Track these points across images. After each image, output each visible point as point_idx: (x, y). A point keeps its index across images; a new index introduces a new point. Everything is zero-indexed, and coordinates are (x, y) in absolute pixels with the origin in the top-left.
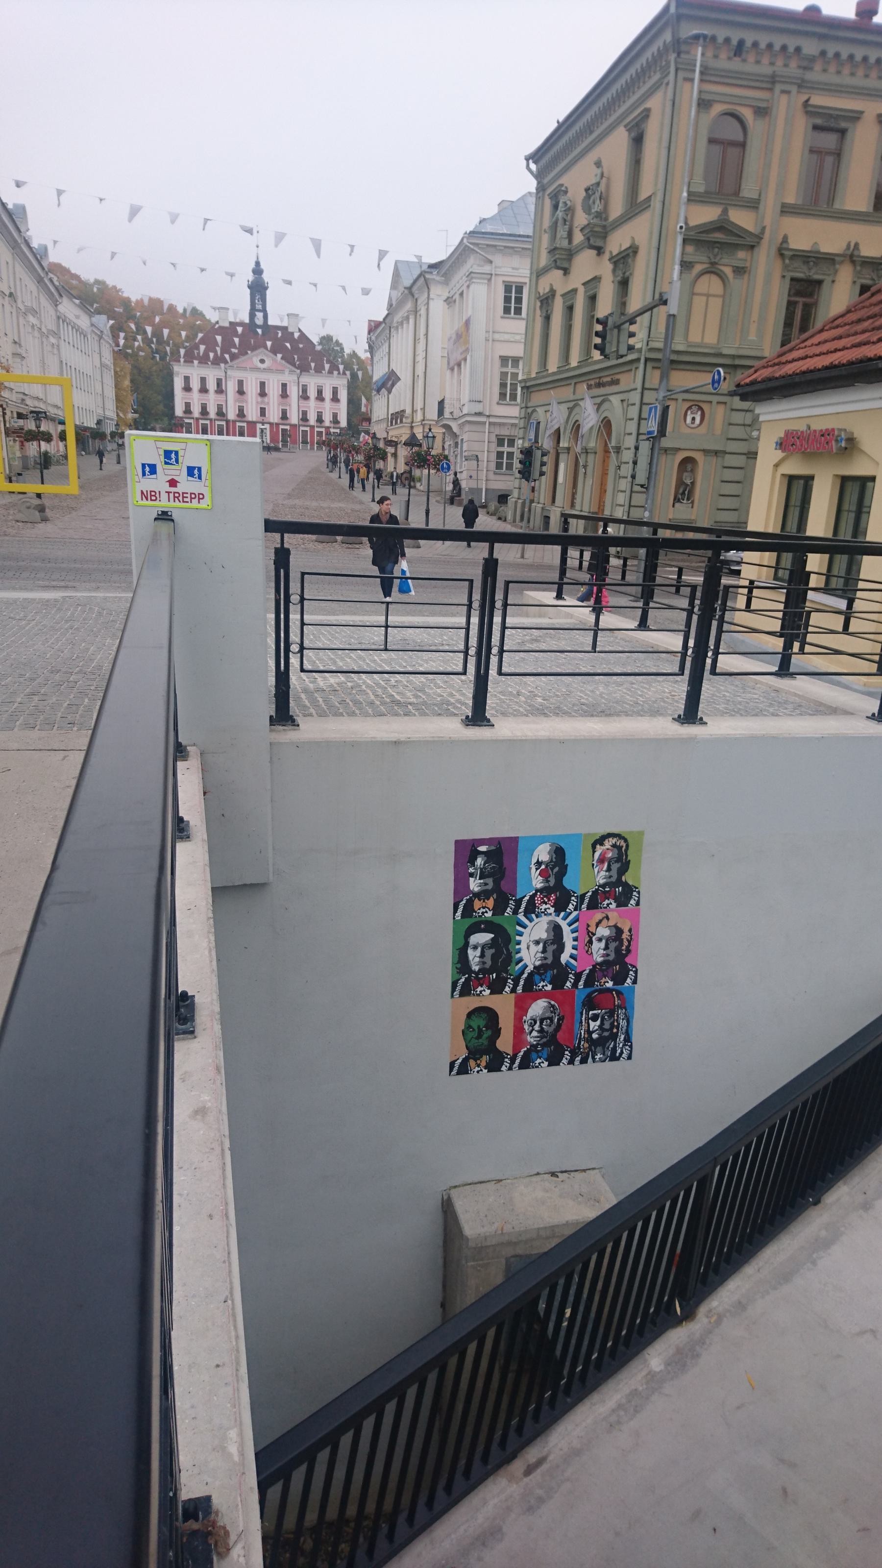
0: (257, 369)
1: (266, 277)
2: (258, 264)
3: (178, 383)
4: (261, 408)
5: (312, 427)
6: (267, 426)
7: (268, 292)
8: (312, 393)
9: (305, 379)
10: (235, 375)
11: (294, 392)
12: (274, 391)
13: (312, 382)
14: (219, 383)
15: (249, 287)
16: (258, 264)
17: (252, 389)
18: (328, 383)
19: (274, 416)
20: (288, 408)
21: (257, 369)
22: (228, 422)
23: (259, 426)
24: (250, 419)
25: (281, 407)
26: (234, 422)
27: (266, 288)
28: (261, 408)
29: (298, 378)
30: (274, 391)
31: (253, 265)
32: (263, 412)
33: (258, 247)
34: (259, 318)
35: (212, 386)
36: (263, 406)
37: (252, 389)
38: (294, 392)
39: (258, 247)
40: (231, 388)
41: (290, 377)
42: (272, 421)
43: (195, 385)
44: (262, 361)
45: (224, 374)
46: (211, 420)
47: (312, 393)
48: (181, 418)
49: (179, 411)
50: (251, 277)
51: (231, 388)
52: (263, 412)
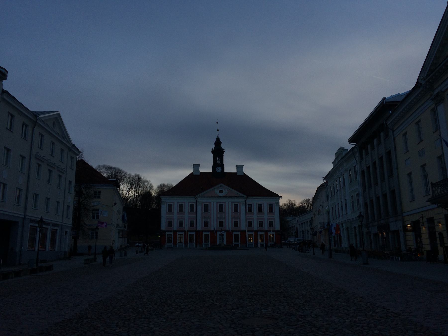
0: (220, 197)
1: (223, 146)
2: (218, 139)
3: (164, 209)
4: (220, 222)
5: (256, 232)
6: (224, 233)
7: (225, 155)
8: (255, 209)
9: (250, 201)
10: (203, 201)
11: (242, 209)
12: (228, 209)
13: (255, 202)
14: (192, 207)
15: (213, 152)
16: (218, 139)
17: (214, 209)
18: (265, 202)
19: (229, 226)
20: (239, 220)
21: (220, 197)
22: (197, 232)
23: (219, 233)
24: (212, 229)
25: (234, 220)
26: (201, 232)
27: (224, 151)
28: (220, 222)
29: (245, 201)
30: (228, 209)
31: (215, 140)
32: (221, 224)
33: (218, 130)
34: (219, 170)
35: (187, 209)
36: (221, 220)
37: (214, 209)
38: (242, 209)
39: (218, 130)
40: (200, 209)
41: (240, 201)
42: (227, 229)
43: (176, 209)
44: (221, 192)
45: (195, 201)
46: (185, 231)
47: (255, 209)
48: (165, 232)
49: (164, 226)
50: (213, 146)
51: (200, 209)
52: (221, 224)
